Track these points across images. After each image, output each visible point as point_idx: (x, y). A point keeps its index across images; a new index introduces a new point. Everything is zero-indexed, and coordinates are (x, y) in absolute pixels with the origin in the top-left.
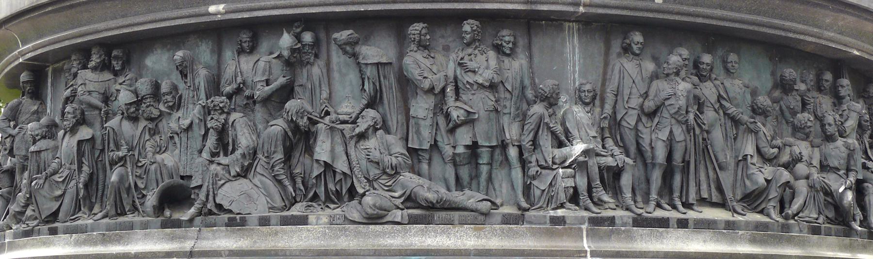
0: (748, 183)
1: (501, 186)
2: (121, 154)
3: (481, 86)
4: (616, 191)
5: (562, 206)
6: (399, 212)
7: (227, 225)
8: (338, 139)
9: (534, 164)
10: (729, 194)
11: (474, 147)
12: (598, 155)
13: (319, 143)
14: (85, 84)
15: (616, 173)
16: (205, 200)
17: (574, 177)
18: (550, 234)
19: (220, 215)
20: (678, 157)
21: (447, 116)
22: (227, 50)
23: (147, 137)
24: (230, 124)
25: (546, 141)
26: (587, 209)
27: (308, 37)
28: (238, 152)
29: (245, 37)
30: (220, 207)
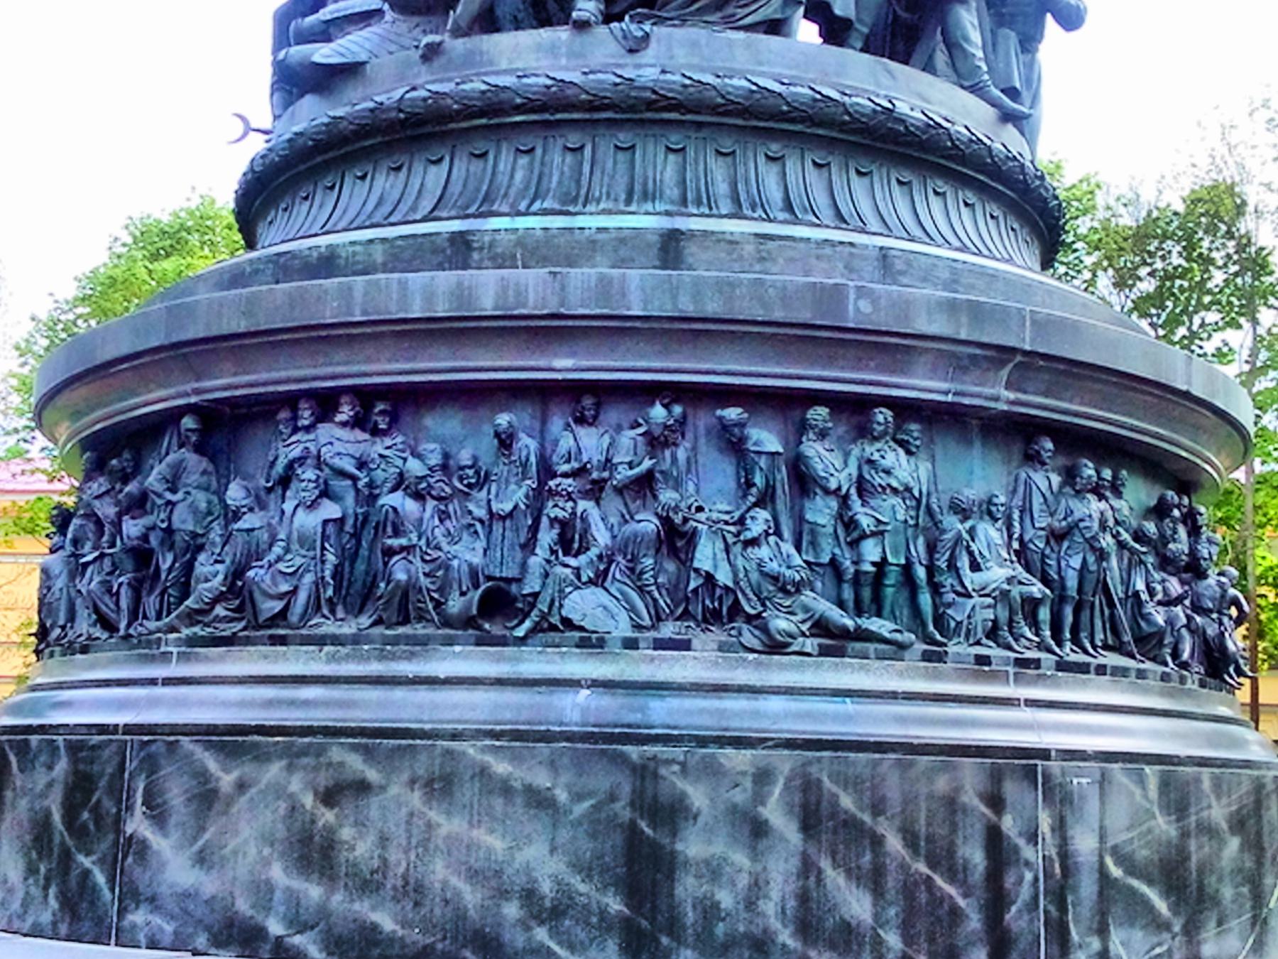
0: (1143, 624)
1: (901, 613)
2: (404, 541)
3: (895, 491)
4: (1035, 625)
6: (809, 641)
7: (577, 646)
9: (948, 588)
10: (1127, 638)
11: (881, 565)
12: (1020, 583)
13: (699, 548)
14: (331, 443)
15: (1031, 605)
16: (546, 610)
17: (995, 606)
18: (978, 677)
19: (562, 632)
21: (850, 524)
22: (555, 418)
23: (437, 522)
24: (579, 514)
26: (1010, 648)
28: (593, 552)
29: (588, 401)
30: (568, 623)
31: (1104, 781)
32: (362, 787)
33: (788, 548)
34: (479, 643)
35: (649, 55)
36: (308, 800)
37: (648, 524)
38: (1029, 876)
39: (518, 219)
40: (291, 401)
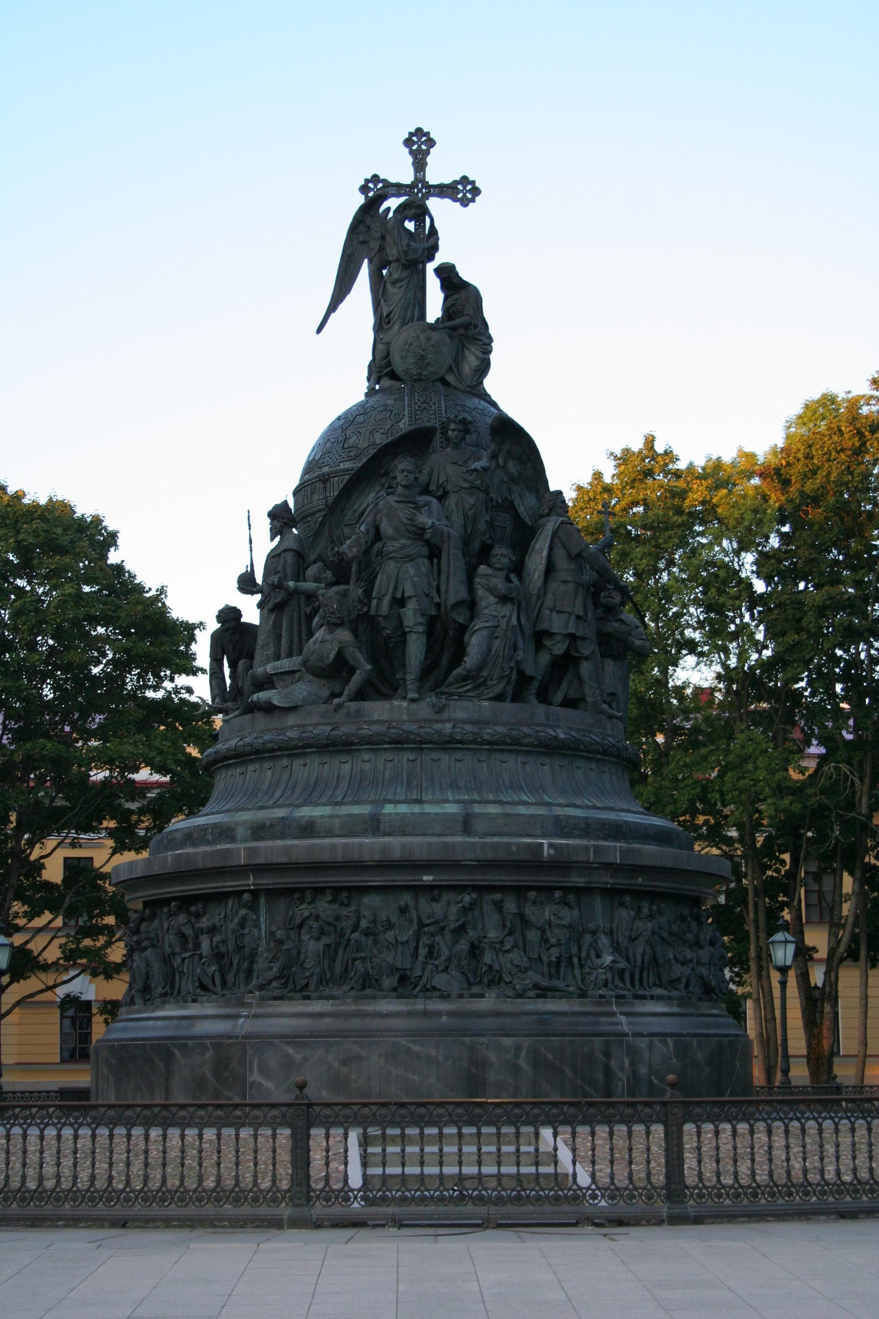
2: (363, 955)
3: (564, 926)
4: (622, 979)
5: (600, 989)
8: (494, 953)
11: (559, 958)
15: (622, 972)
18: (600, 1004)
20: (646, 962)
21: (547, 941)
25: (593, 954)
27: (474, 896)
30: (434, 988)
31: (651, 1046)
32: (359, 1058)
33: (522, 953)
34: (398, 997)
35: (445, 715)
36: (336, 1064)
37: (463, 946)
38: (620, 1084)
39: (399, 806)
40: (302, 890)
